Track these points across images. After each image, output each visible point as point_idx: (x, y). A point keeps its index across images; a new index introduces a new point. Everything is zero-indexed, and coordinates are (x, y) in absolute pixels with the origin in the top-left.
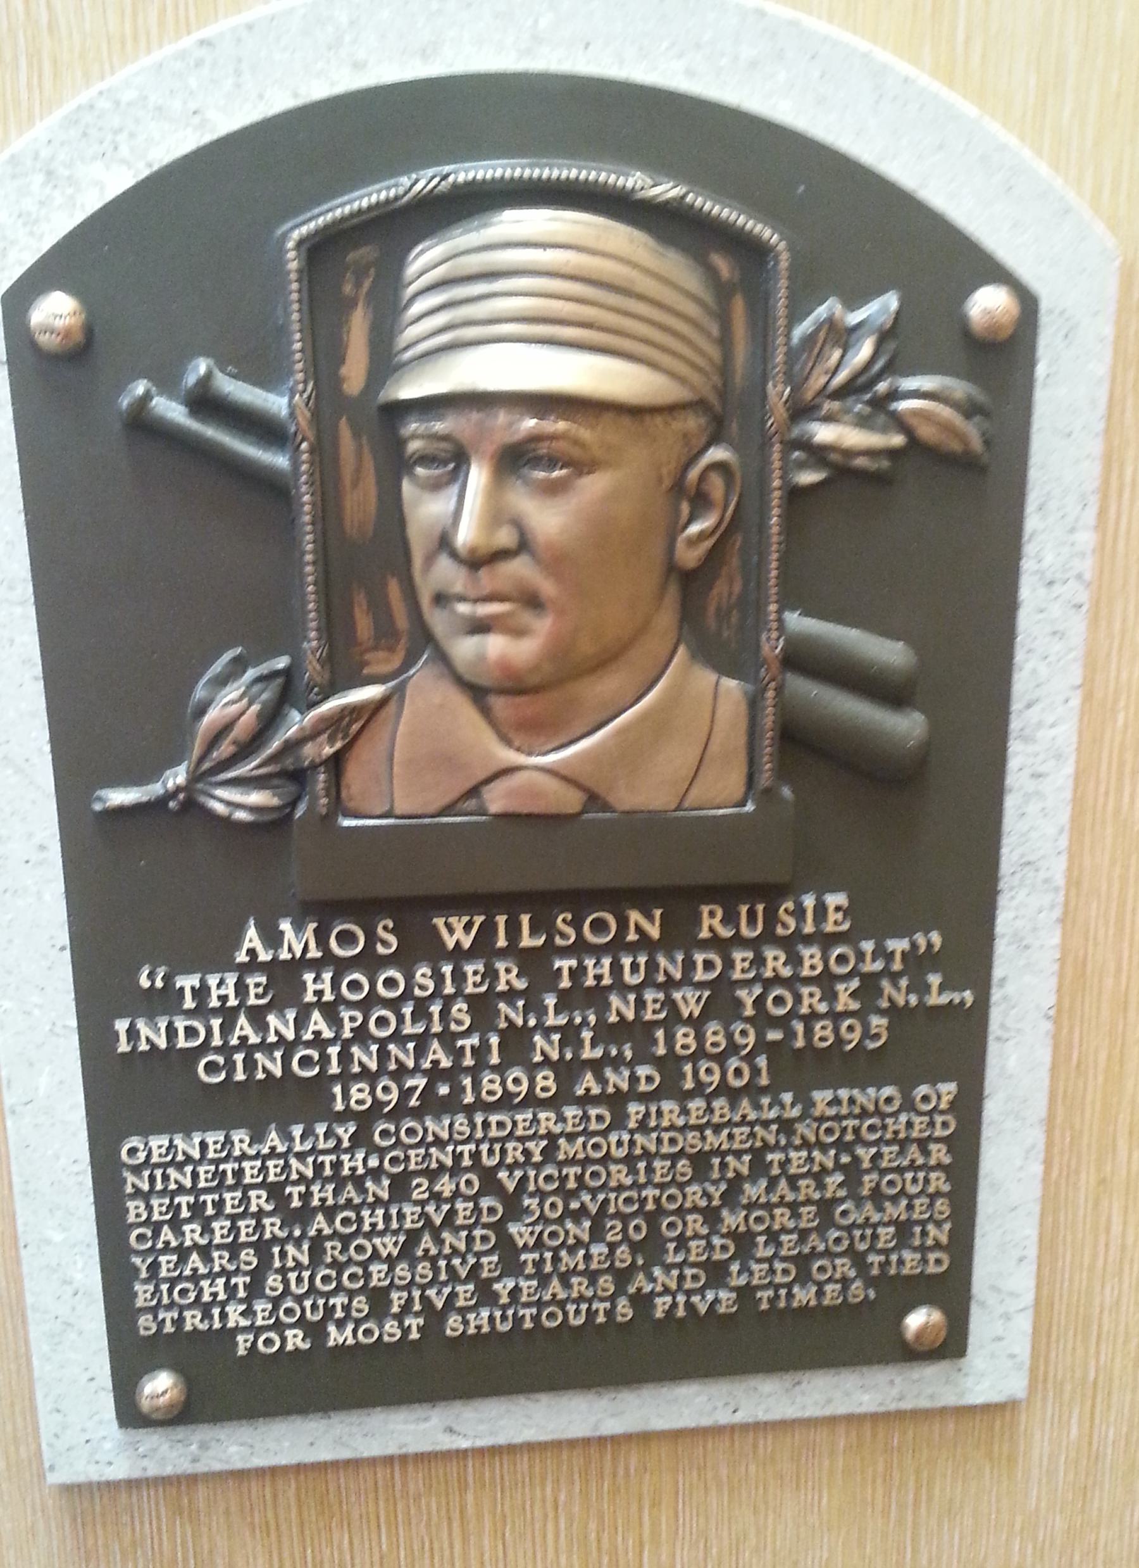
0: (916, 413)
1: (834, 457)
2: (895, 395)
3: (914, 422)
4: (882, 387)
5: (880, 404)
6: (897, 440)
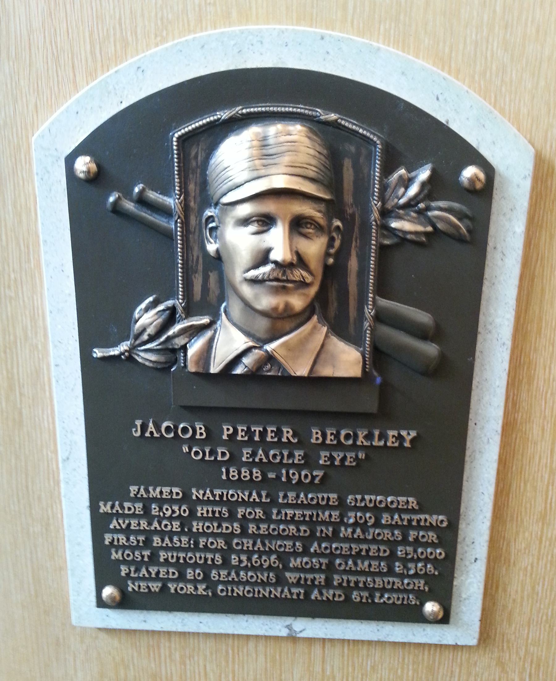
0: (437, 217)
1: (400, 234)
2: (428, 209)
3: (435, 220)
4: (422, 205)
5: (420, 212)
6: (429, 229)
